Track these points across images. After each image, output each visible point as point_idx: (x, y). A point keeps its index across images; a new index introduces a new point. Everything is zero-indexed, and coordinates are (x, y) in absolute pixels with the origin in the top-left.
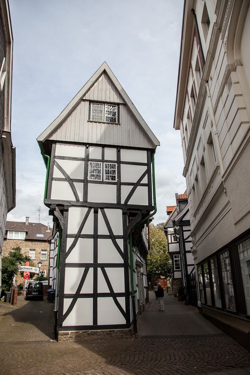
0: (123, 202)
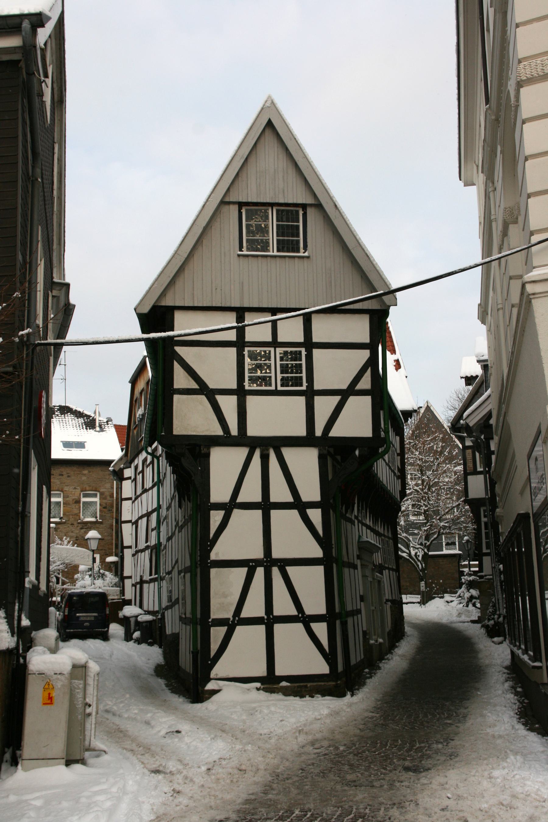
0: (319, 432)
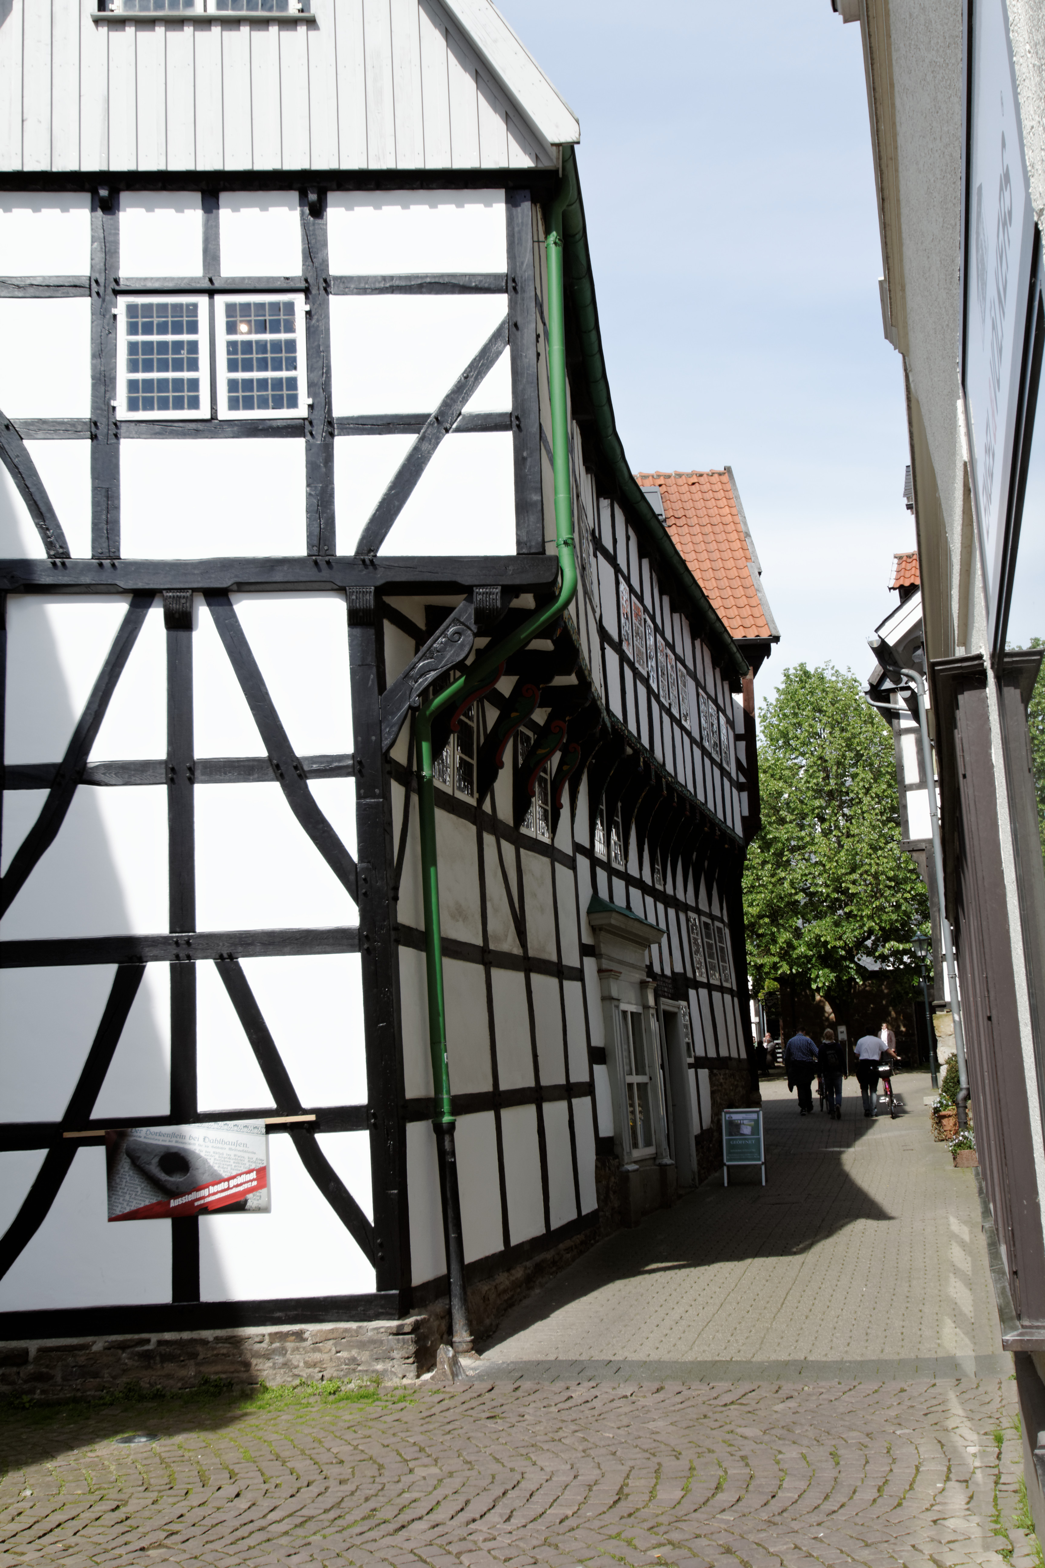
0: (346, 545)
